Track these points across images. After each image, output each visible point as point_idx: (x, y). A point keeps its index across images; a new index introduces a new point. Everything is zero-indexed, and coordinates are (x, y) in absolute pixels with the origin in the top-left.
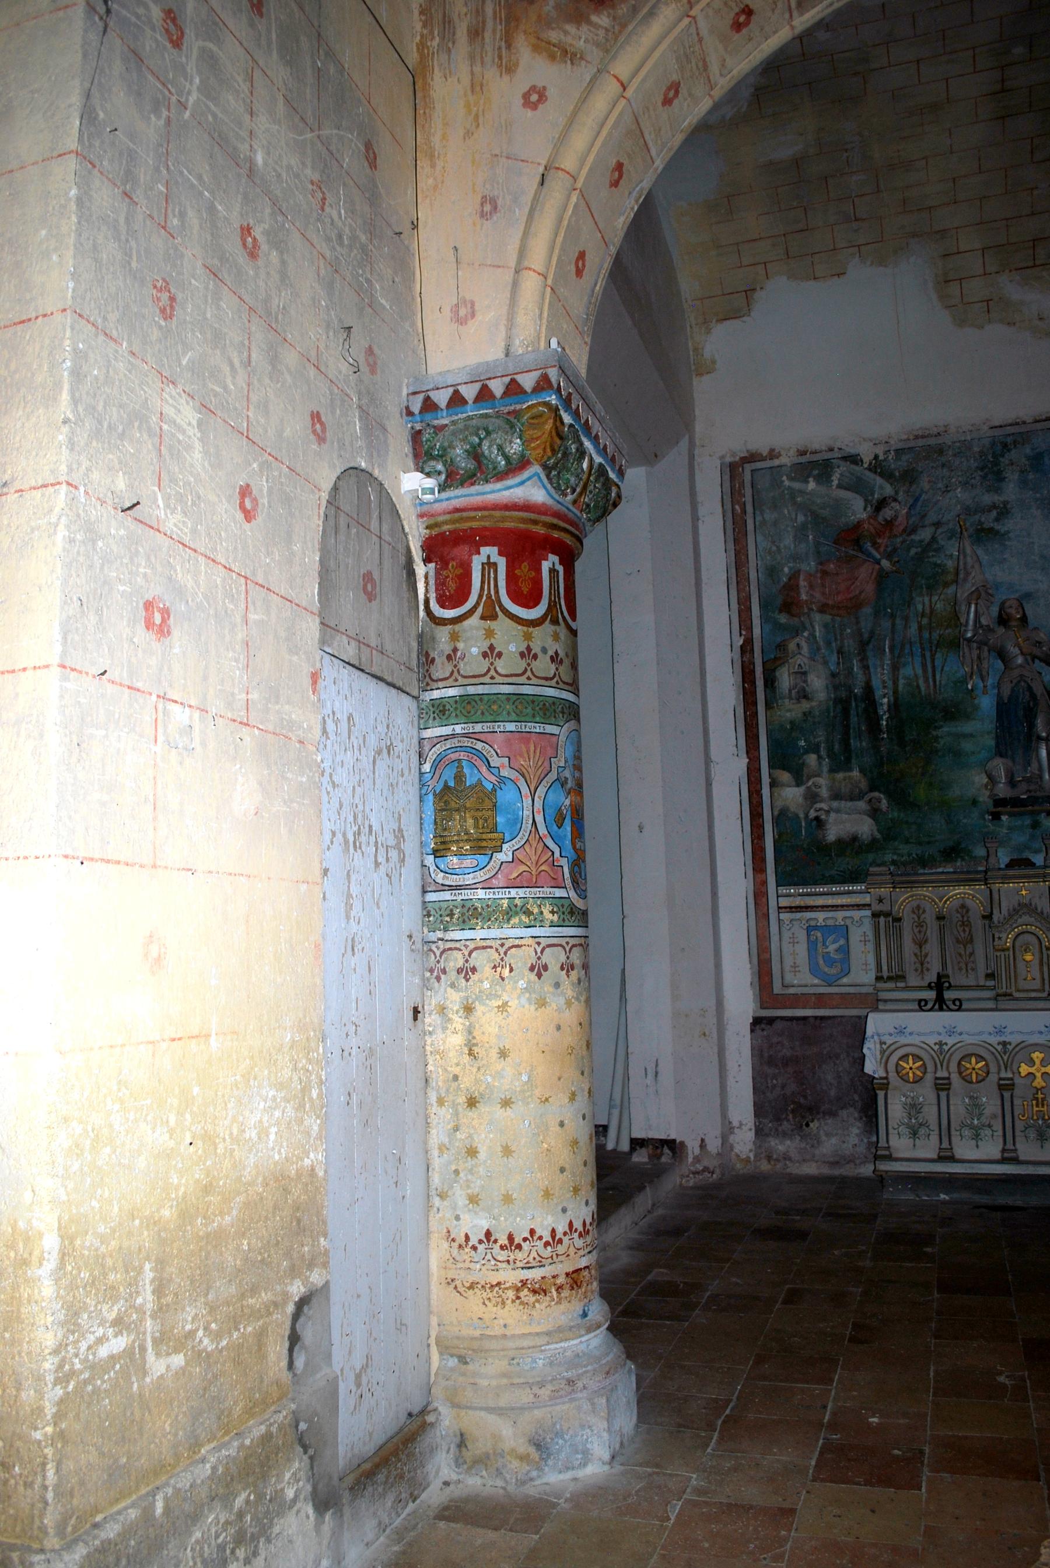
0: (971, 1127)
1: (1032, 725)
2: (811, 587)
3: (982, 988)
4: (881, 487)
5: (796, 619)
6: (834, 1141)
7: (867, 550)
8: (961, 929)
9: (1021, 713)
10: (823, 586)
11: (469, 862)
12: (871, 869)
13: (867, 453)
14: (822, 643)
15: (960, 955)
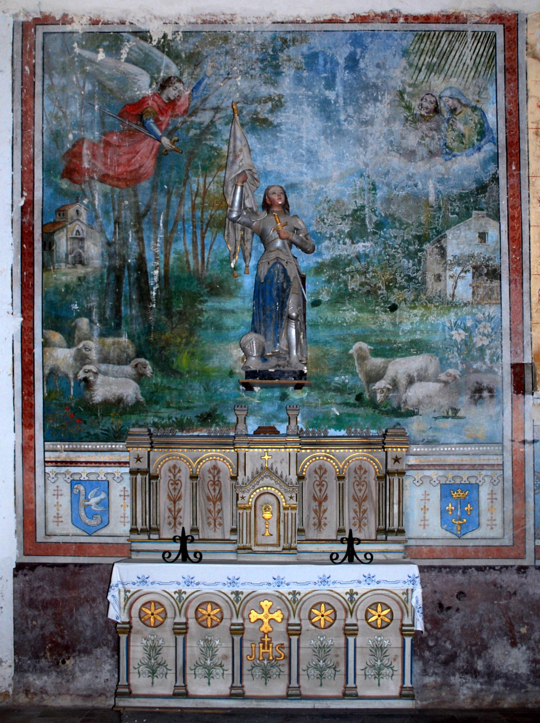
0: (205, 666)
1: (283, 305)
2: (94, 156)
3: (228, 541)
4: (167, 67)
5: (78, 186)
6: (87, 676)
7: (150, 126)
8: (211, 488)
9: (275, 293)
10: (105, 156)
12: (132, 430)
14: (100, 212)
15: (210, 511)
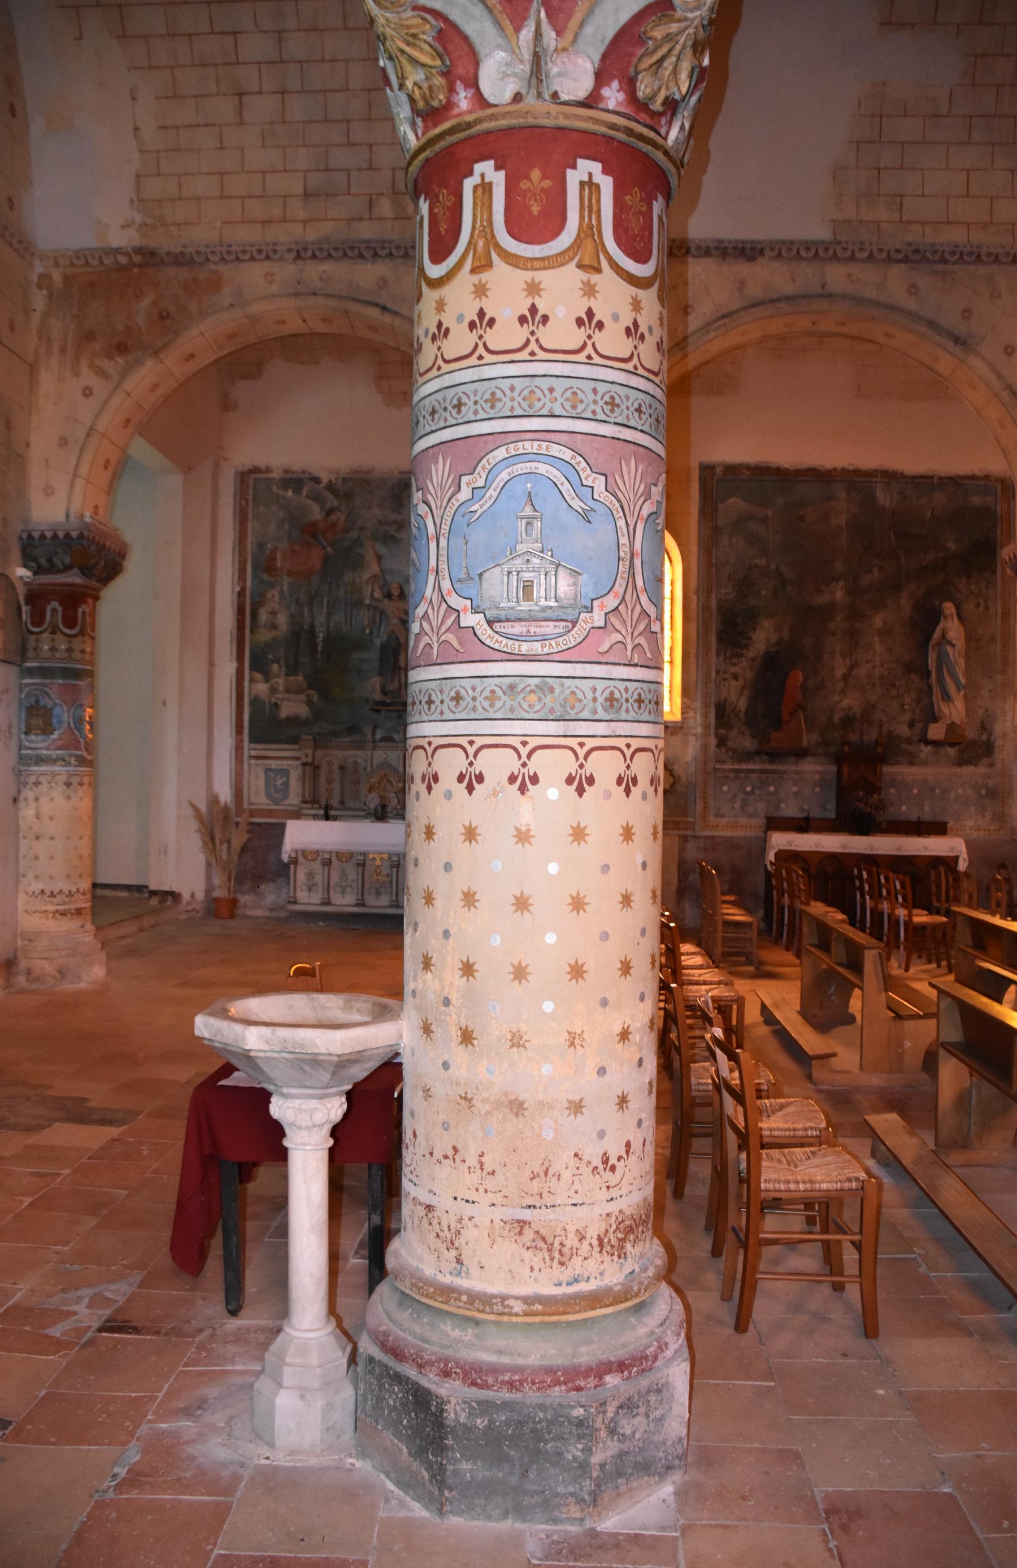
11: (40, 738)
14: (286, 594)
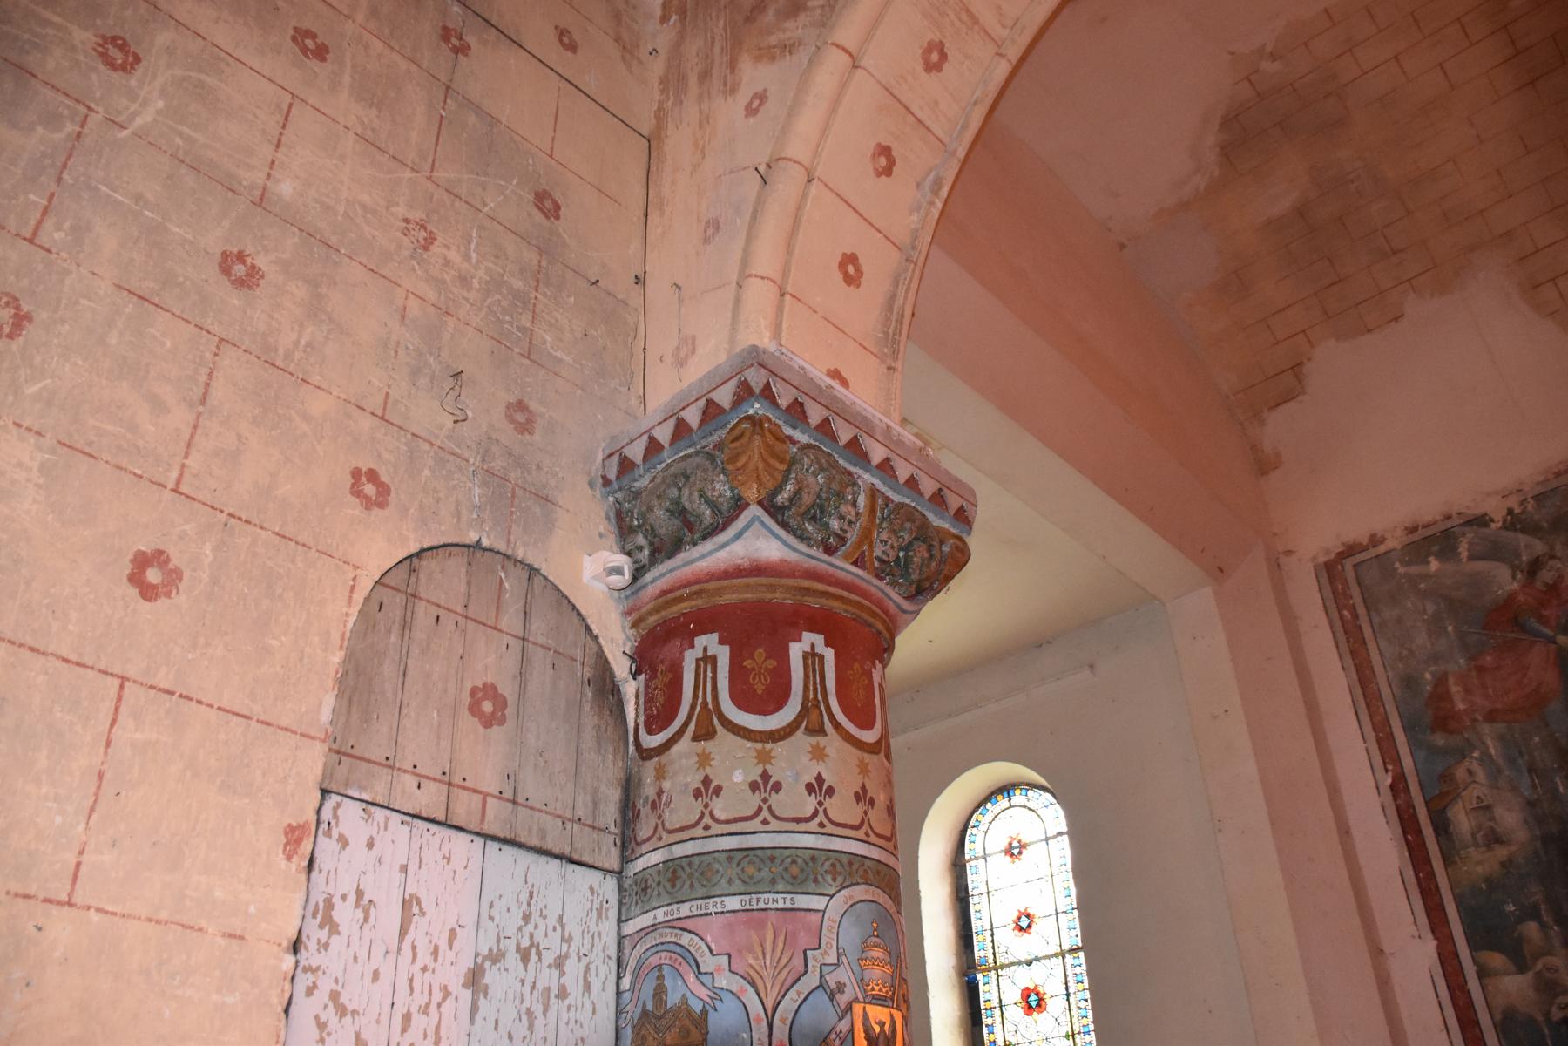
2: (1467, 691)
13: (1496, 509)
14: (1501, 762)
